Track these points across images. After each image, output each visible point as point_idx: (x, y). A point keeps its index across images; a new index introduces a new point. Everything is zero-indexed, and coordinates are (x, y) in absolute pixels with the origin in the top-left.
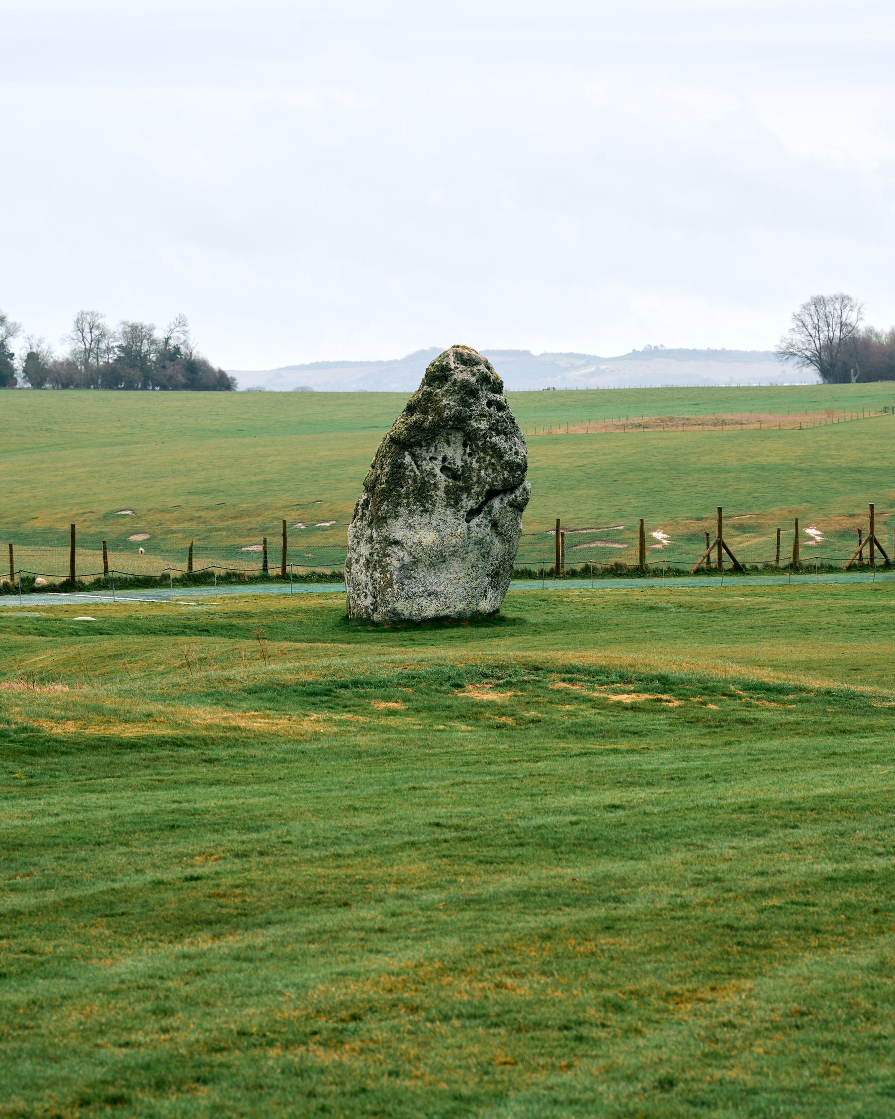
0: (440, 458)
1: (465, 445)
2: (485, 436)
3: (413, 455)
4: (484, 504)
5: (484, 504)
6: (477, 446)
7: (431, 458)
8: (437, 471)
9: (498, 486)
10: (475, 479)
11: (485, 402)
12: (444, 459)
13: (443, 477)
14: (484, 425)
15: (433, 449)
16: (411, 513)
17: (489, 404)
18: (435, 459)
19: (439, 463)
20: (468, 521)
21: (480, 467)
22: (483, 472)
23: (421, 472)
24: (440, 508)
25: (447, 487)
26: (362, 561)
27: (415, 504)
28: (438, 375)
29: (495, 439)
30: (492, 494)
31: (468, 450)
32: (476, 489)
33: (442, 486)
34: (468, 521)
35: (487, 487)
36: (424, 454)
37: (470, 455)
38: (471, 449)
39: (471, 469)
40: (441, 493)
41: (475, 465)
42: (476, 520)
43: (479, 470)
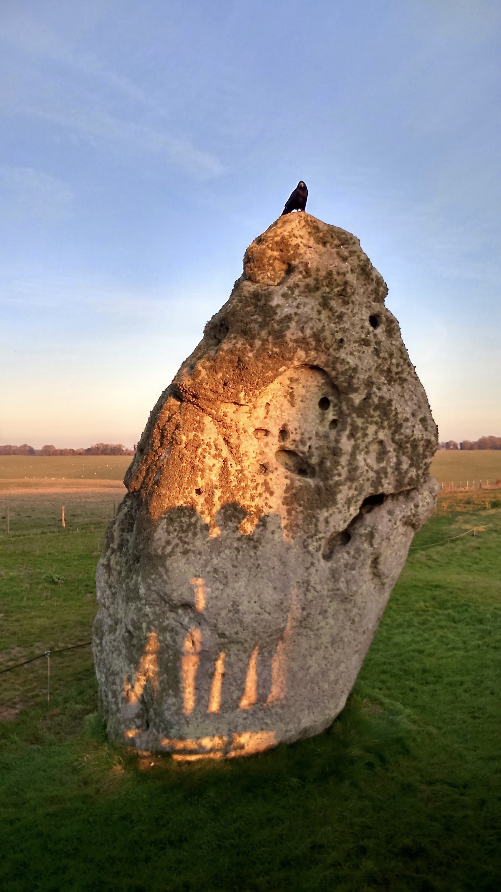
0: (275, 431)
2: (369, 384)
4: (358, 518)
6: (350, 402)
10: (344, 472)
11: (366, 314)
17: (374, 321)
21: (356, 447)
22: (360, 457)
25: (288, 489)
26: (121, 632)
29: (385, 392)
30: (374, 501)
31: (331, 415)
37: (334, 423)
38: (340, 412)
39: (336, 452)
41: (346, 444)
42: (343, 556)
43: (353, 455)
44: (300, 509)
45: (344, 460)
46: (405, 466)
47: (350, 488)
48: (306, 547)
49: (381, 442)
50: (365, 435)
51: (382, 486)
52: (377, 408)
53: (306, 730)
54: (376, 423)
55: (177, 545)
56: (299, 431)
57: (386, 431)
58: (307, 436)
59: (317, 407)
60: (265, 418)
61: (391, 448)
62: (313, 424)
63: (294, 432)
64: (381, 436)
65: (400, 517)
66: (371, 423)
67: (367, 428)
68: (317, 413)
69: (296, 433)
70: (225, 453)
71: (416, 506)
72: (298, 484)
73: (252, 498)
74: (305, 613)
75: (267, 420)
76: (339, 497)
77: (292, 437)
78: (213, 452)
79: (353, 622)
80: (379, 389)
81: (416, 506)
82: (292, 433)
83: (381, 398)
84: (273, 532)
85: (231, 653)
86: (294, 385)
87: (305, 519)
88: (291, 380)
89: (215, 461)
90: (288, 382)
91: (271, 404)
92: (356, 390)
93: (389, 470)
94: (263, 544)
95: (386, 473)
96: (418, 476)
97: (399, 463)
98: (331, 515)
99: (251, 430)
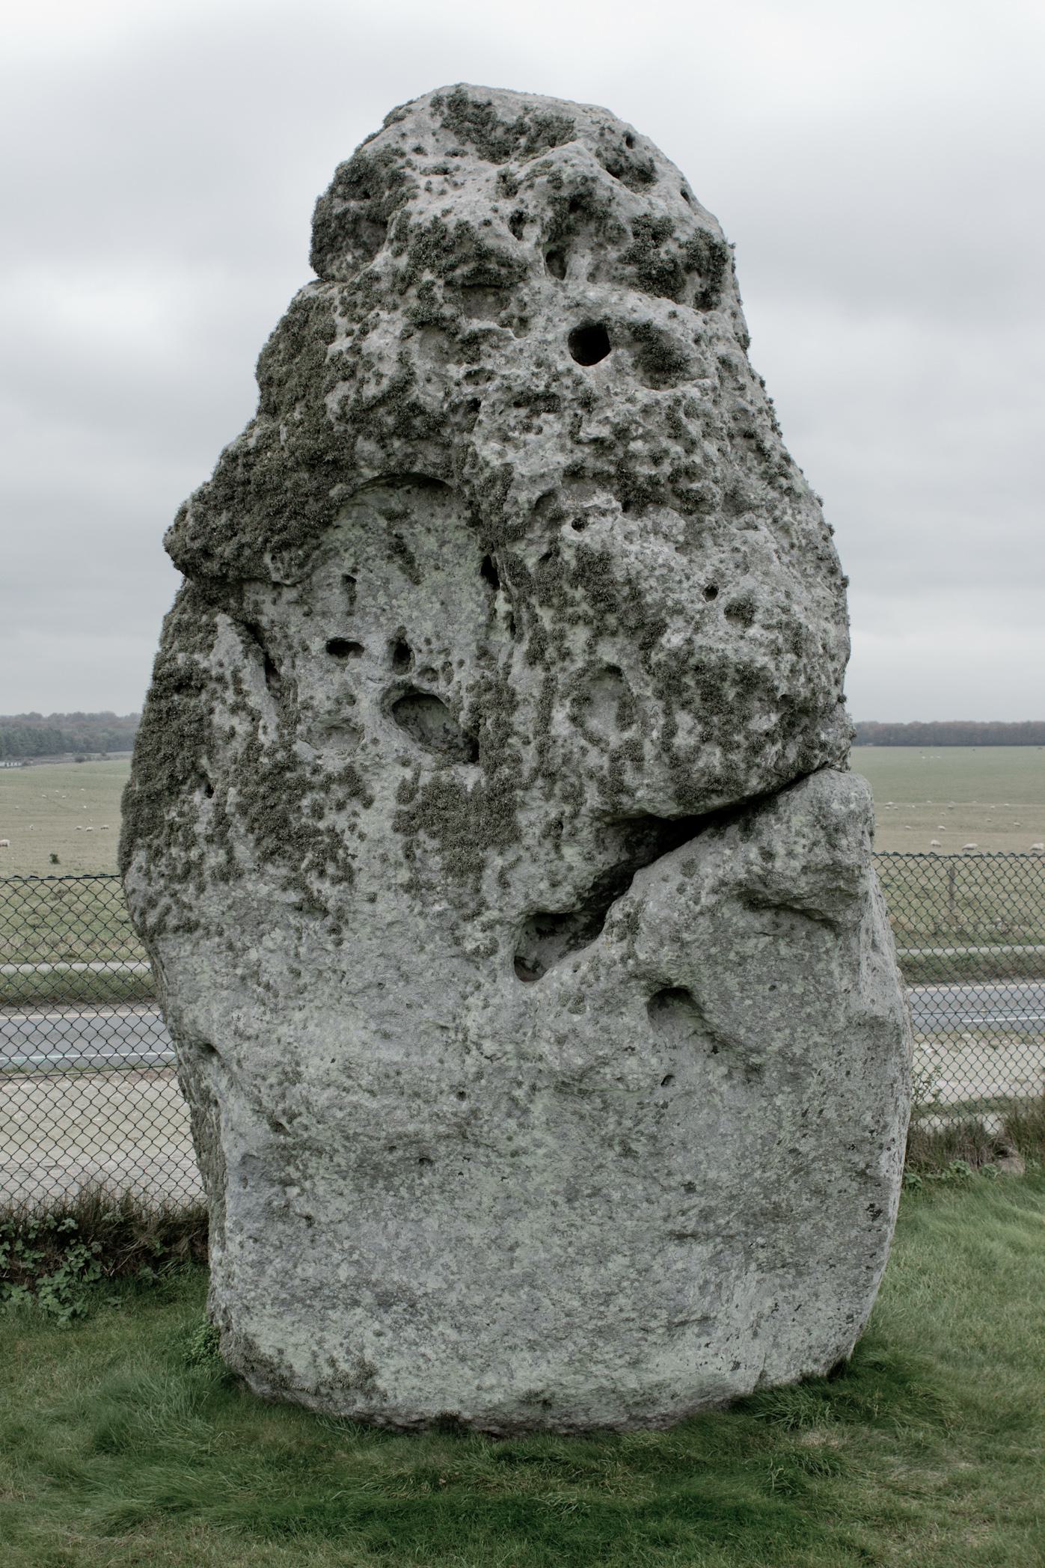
0: (376, 644)
1: (489, 572)
3: (253, 632)
5: (614, 884)
7: (340, 648)
8: (367, 710)
9: (650, 792)
10: (529, 757)
12: (401, 652)
13: (395, 740)
14: (540, 454)
15: (335, 598)
16: (255, 919)
18: (356, 648)
19: (371, 676)
20: (527, 969)
21: (548, 684)
22: (560, 714)
23: (288, 721)
24: (381, 903)
25: (406, 793)
27: (259, 871)
28: (359, 209)
32: (535, 813)
33: (384, 787)
34: (527, 969)
35: (593, 798)
36: (296, 624)
40: (377, 821)
41: (525, 680)
42: (562, 974)
44: (433, 844)
45: (524, 719)
46: (683, 740)
47: (548, 797)
48: (457, 941)
49: (614, 671)
50: (565, 655)
51: (630, 792)
52: (577, 578)
53: (530, 1399)
54: (588, 622)
55: (168, 910)
56: (435, 645)
57: (621, 640)
58: (454, 658)
59: (480, 582)
60: (350, 614)
61: (642, 687)
62: (471, 626)
63: (424, 648)
64: (608, 653)
65: (709, 883)
66: (574, 621)
67: (561, 636)
68: (482, 597)
69: (431, 652)
70: (258, 697)
71: (768, 855)
72: (426, 778)
73: (318, 812)
74: (465, 1105)
75: (356, 620)
76: (522, 818)
77: (419, 660)
78: (230, 696)
79: (628, 1152)
80: (578, 526)
81: (768, 855)
82: (420, 651)
83: (581, 551)
84: (372, 899)
85: (310, 1171)
86: (402, 529)
87: (449, 869)
88: (392, 517)
89: (235, 721)
90: (383, 523)
91: (358, 577)
92: (516, 534)
93: (649, 750)
94: (354, 925)
95: (638, 760)
96: (730, 767)
97: (670, 732)
98: (513, 866)
99: (317, 645)
